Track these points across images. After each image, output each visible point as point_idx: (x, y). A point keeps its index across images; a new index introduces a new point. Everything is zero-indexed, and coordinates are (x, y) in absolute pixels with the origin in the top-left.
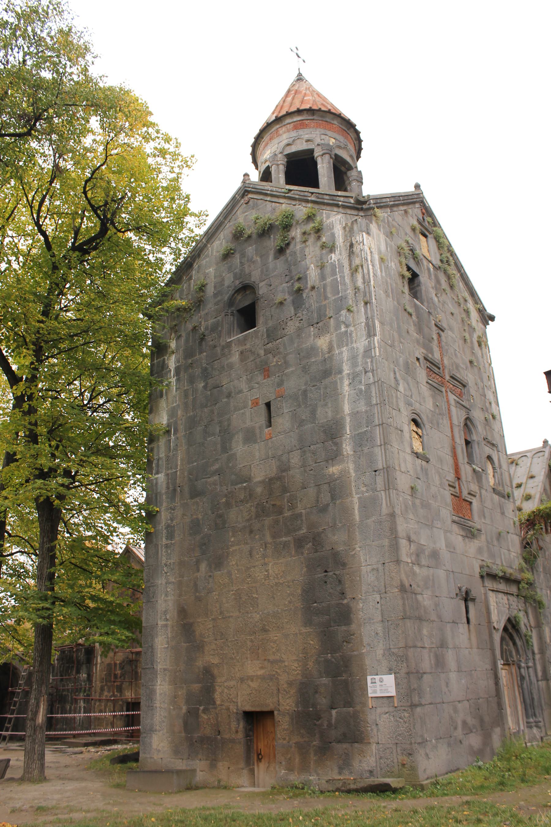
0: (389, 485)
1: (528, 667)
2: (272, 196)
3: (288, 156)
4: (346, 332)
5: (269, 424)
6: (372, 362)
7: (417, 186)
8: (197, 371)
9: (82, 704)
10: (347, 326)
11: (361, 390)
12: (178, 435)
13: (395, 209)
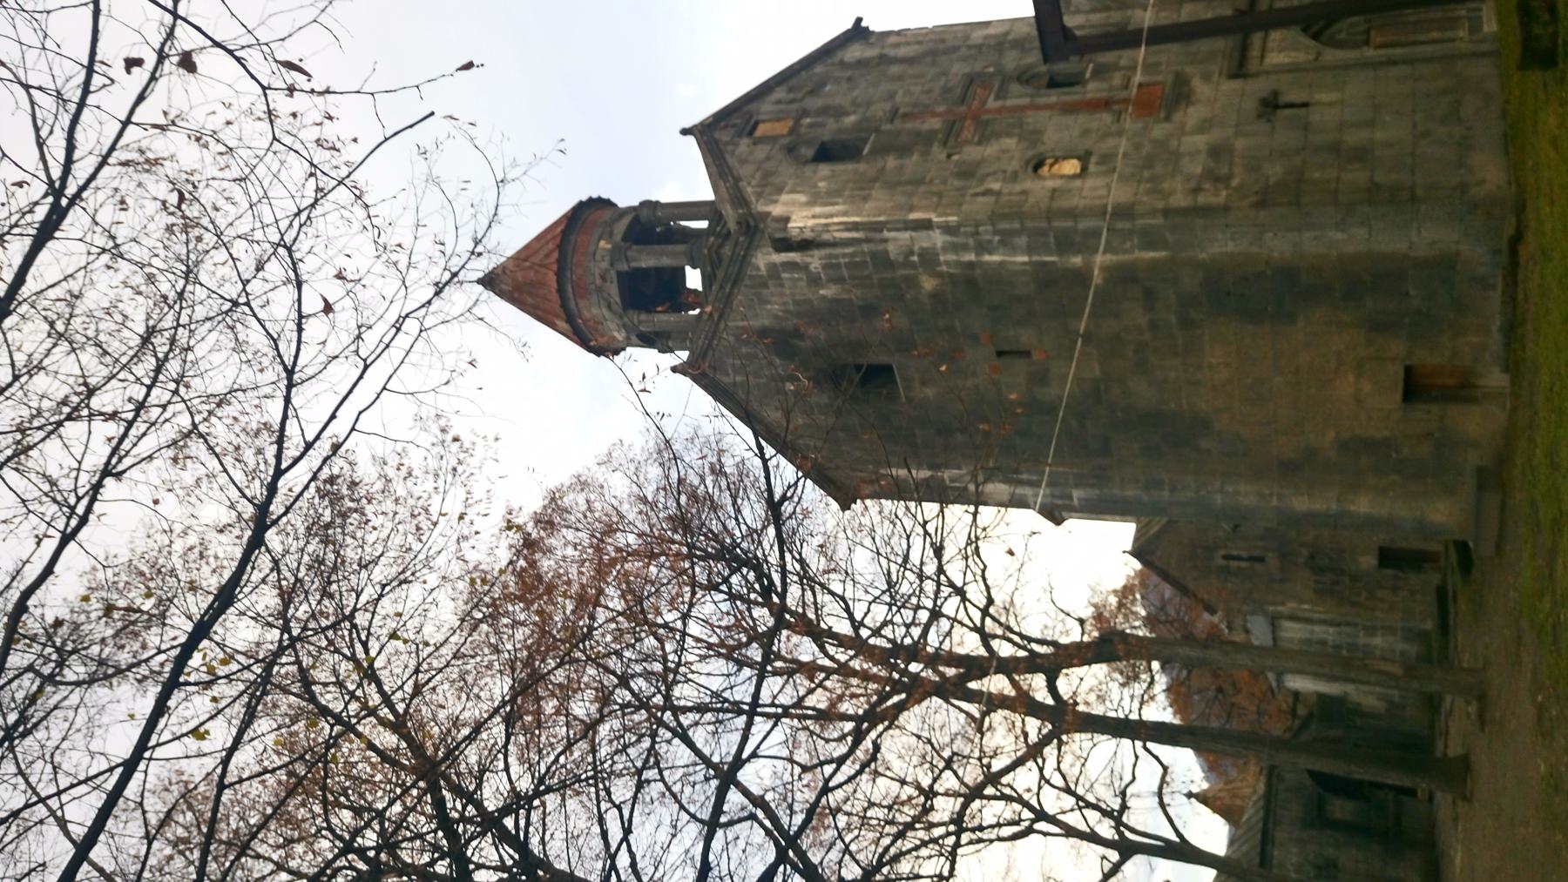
3: (625, 308)
4: (920, 255)
5: (1026, 354)
7: (685, 132)
9: (1378, 641)
10: (912, 253)
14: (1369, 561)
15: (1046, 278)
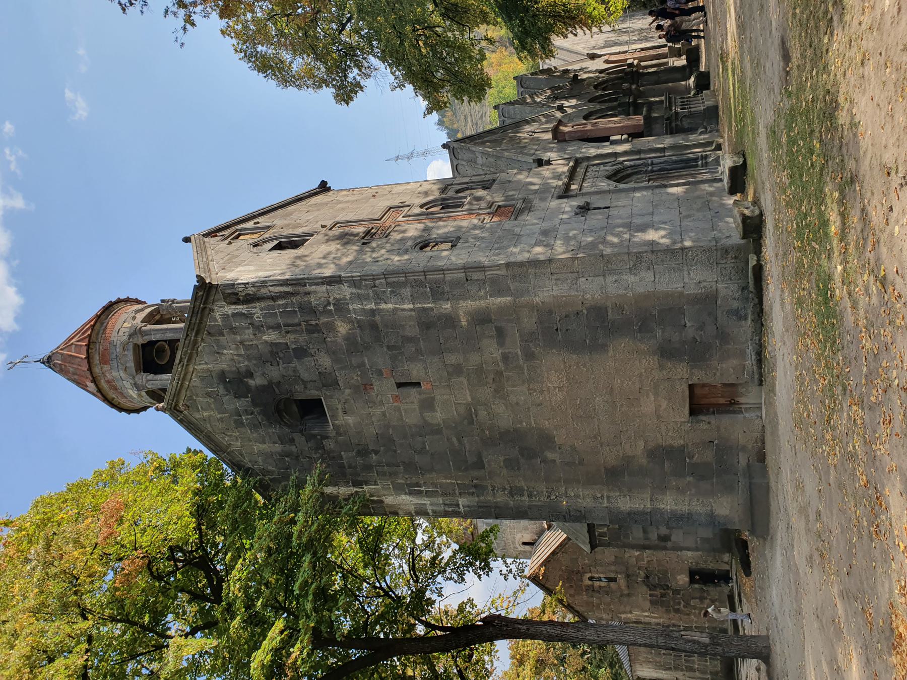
0: (481, 268)
1: (652, 164)
2: (184, 379)
4: (334, 304)
6: (365, 280)
7: (187, 240)
8: (359, 460)
11: (392, 292)
12: (422, 482)
13: (210, 258)
14: (683, 579)
15: (428, 323)
